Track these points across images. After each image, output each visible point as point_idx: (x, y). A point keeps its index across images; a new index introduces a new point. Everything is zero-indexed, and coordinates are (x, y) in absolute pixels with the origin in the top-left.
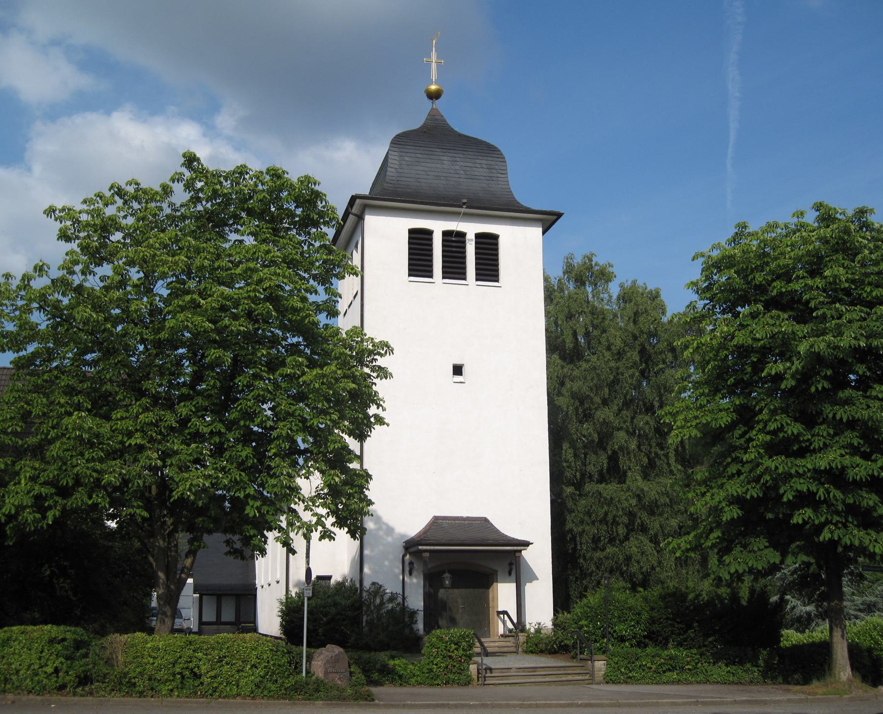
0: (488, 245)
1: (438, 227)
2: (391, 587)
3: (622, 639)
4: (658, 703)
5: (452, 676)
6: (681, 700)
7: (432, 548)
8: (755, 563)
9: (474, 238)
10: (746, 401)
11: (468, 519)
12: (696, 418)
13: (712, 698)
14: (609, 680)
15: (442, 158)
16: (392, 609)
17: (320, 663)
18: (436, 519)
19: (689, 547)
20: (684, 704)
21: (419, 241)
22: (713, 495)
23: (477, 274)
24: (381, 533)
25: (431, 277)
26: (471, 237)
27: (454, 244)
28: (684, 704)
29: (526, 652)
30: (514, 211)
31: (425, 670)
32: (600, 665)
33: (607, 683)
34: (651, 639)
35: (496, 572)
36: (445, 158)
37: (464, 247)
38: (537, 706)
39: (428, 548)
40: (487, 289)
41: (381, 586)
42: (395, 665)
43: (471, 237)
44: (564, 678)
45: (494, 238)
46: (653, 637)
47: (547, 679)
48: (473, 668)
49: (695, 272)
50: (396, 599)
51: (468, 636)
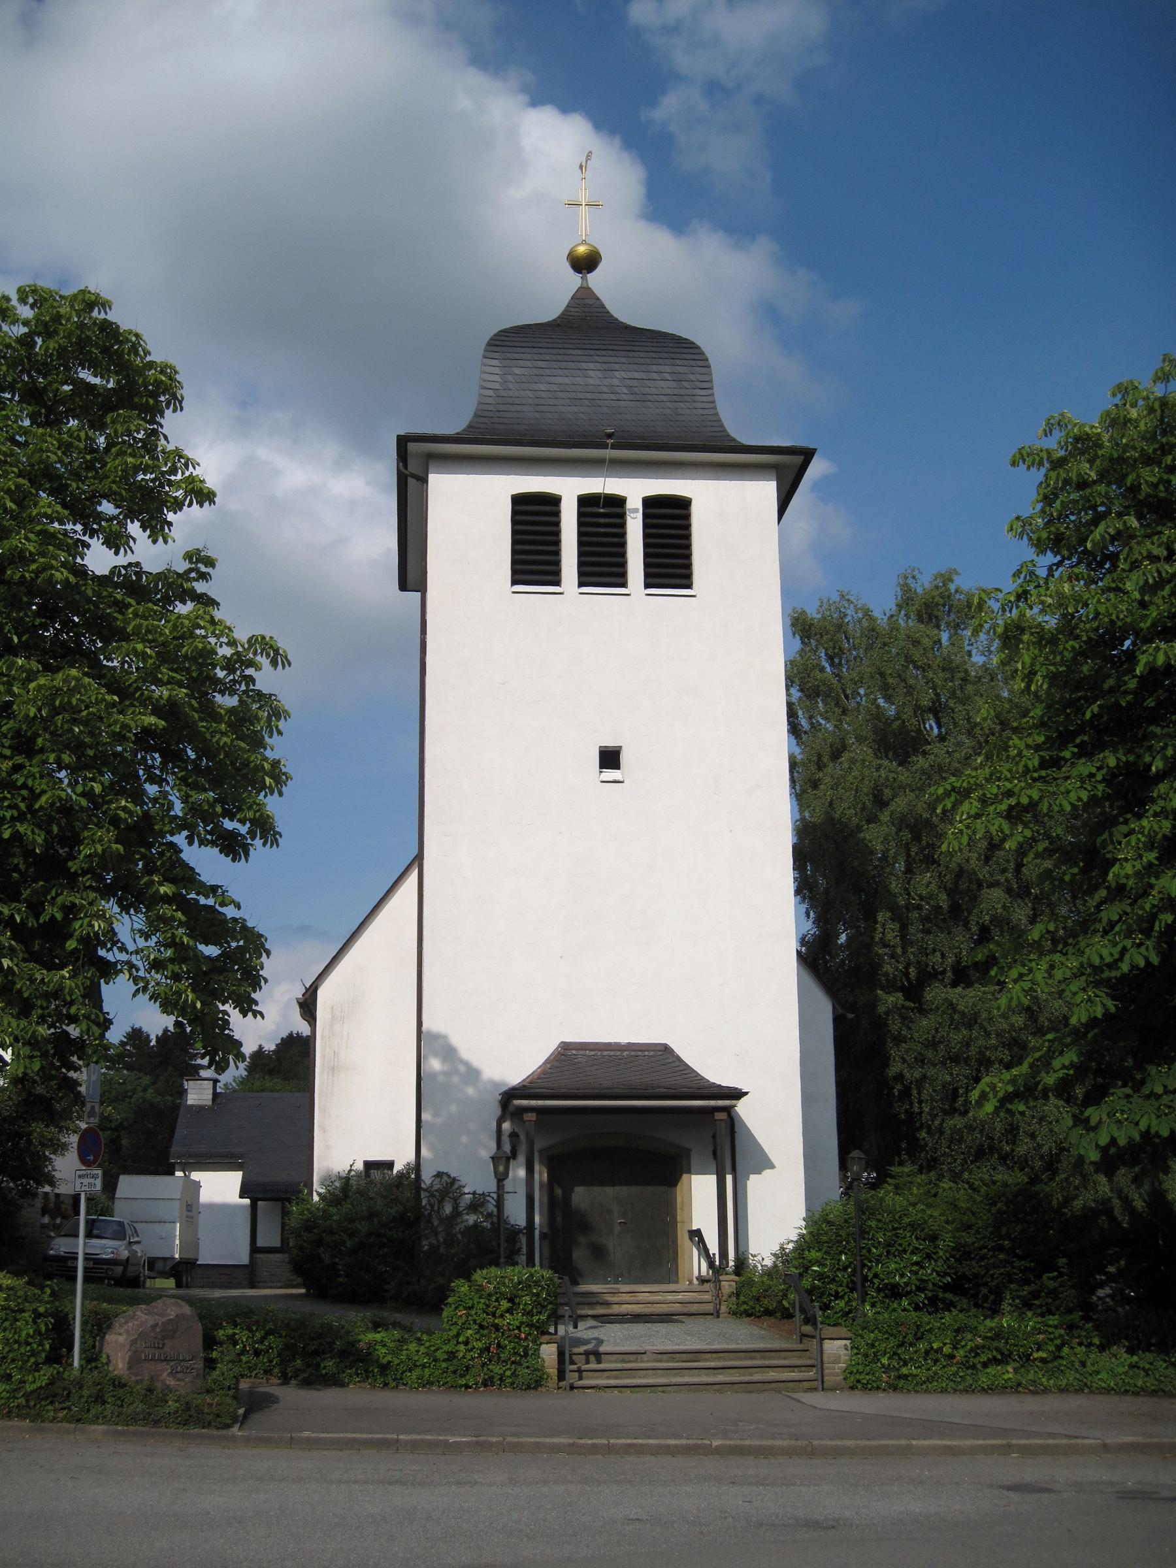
0: (670, 523)
1: (569, 488)
2: (477, 1179)
3: (894, 1292)
4: (910, 1447)
5: (497, 1369)
6: (969, 1442)
7: (540, 1103)
8: (1155, 1122)
9: (640, 506)
10: (1131, 758)
11: (630, 1047)
12: (1009, 794)
13: (1051, 1435)
14: (857, 1382)
15: (584, 365)
16: (476, 1225)
17: (121, 1339)
18: (565, 1047)
19: (1010, 1089)
20: (974, 1451)
21: (533, 520)
22: (1052, 967)
23: (647, 575)
24: (456, 1079)
25: (557, 583)
26: (634, 503)
27: (602, 520)
28: (974, 1451)
29: (734, 1313)
30: (724, 454)
31: (440, 1355)
32: (836, 1349)
33: (852, 1388)
34: (963, 1292)
35: (688, 1151)
36: (591, 366)
37: (623, 525)
38: (610, 1450)
39: (533, 1103)
40: (668, 602)
41: (454, 1180)
42: (371, 1345)
43: (634, 503)
44: (756, 1378)
45: (681, 505)
46: (966, 1287)
47: (721, 1378)
48: (548, 1352)
49: (1024, 492)
50: (483, 1204)
51: (537, 1283)
